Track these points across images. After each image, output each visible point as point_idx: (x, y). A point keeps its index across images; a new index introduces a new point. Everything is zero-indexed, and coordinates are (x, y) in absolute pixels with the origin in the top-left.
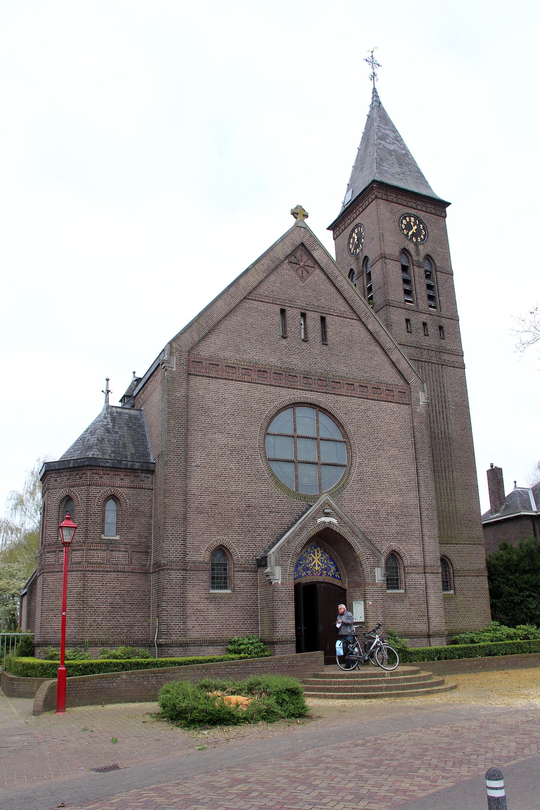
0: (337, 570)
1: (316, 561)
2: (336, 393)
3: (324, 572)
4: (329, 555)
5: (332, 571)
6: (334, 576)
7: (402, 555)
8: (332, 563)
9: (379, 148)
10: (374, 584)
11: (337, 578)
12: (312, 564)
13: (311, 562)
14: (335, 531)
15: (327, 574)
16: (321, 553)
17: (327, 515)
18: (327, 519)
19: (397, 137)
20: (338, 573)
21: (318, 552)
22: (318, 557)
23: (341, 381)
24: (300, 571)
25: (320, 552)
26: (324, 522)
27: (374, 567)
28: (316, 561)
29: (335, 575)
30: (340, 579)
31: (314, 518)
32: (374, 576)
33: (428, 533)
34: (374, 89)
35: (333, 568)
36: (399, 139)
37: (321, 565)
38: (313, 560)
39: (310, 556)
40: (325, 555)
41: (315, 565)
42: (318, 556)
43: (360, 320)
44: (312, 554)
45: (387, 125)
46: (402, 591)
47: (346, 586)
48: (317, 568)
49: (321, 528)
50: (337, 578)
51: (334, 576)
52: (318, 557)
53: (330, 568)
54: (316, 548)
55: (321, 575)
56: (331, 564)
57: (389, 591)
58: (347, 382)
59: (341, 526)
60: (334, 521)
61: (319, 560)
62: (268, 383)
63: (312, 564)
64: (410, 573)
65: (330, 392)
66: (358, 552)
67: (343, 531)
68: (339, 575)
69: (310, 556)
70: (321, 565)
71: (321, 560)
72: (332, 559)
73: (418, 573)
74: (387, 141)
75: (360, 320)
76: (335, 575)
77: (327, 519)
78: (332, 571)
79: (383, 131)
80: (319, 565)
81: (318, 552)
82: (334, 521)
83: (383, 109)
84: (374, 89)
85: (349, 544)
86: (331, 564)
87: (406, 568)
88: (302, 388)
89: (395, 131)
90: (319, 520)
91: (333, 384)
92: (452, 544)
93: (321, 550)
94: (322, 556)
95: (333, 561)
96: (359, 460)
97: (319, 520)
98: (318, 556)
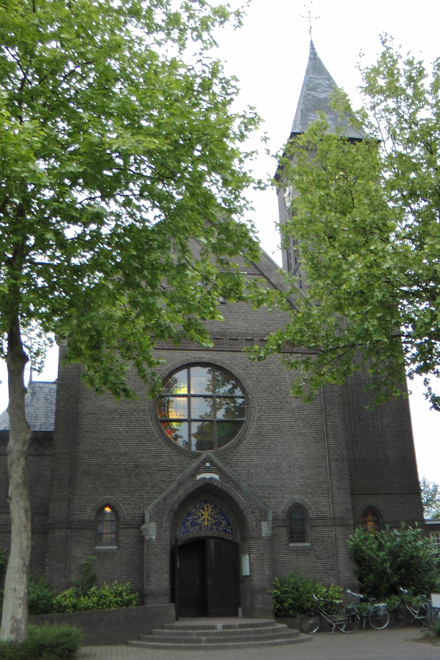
0: (229, 524)
1: (206, 516)
2: (233, 349)
3: (215, 527)
4: (220, 510)
5: (223, 526)
6: (225, 531)
7: (307, 508)
8: (223, 518)
9: (308, 99)
10: (260, 537)
11: (229, 533)
12: (201, 520)
13: (199, 518)
14: (217, 487)
15: (217, 529)
16: (212, 508)
17: (208, 470)
18: (208, 476)
19: (331, 84)
20: (229, 527)
21: (208, 507)
22: (208, 512)
23: (239, 338)
24: (187, 527)
25: (210, 507)
26: (204, 479)
27: (260, 521)
28: (206, 516)
29: (226, 529)
30: (232, 534)
31: (193, 475)
32: (260, 530)
33: (337, 484)
34: (311, 42)
35: (224, 523)
36: (333, 86)
37: (211, 519)
38: (202, 515)
39: (199, 512)
40: (215, 510)
41: (204, 520)
42: (207, 511)
43: (263, 274)
44: (201, 510)
45: (320, 74)
46: (307, 544)
47: (238, 540)
48: (206, 523)
49: (201, 484)
50: (229, 533)
51: (225, 531)
52: (208, 512)
53: (220, 522)
54: (205, 503)
55: (210, 529)
56: (222, 519)
57: (292, 545)
58: (246, 338)
59: (224, 481)
60: (216, 476)
61: (208, 515)
62: (160, 347)
63: (201, 520)
64: (316, 526)
65: (227, 349)
66: (241, 506)
67: (227, 486)
68: (231, 529)
69: (199, 512)
70: (211, 519)
71: (211, 515)
72: (222, 514)
73: (326, 526)
74: (319, 90)
75: (263, 274)
76: (226, 529)
77: (208, 476)
78: (223, 526)
79: (316, 81)
80: (208, 520)
81: (208, 507)
82: (216, 476)
83: (319, 59)
84: (311, 42)
85: (232, 499)
86: (222, 519)
87: (312, 521)
88: (196, 349)
89: (329, 78)
90: (199, 477)
91: (231, 341)
92: (381, 494)
93: (211, 505)
94: (212, 512)
95: (224, 516)
96: (257, 414)
97: (199, 477)
98: (207, 511)
